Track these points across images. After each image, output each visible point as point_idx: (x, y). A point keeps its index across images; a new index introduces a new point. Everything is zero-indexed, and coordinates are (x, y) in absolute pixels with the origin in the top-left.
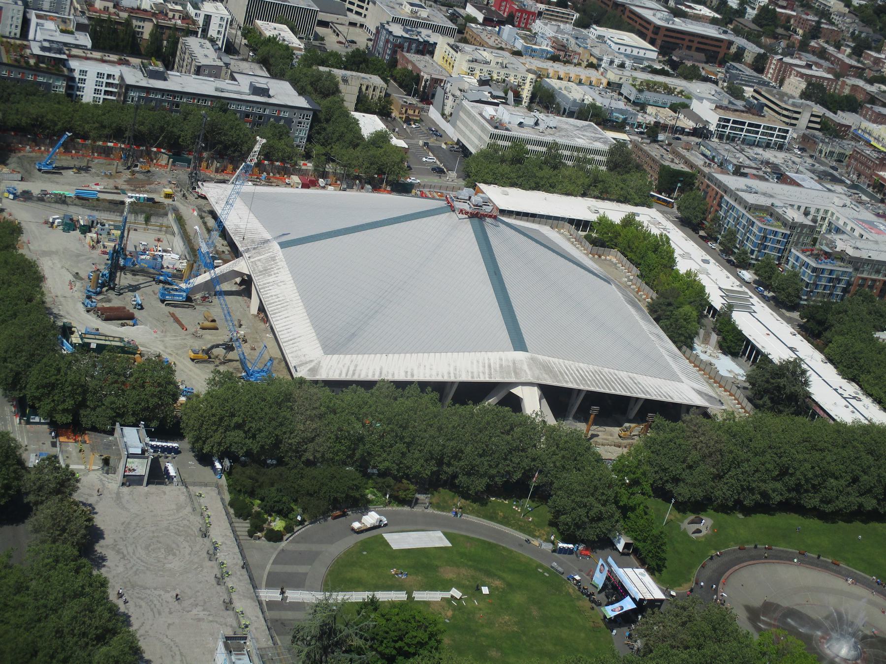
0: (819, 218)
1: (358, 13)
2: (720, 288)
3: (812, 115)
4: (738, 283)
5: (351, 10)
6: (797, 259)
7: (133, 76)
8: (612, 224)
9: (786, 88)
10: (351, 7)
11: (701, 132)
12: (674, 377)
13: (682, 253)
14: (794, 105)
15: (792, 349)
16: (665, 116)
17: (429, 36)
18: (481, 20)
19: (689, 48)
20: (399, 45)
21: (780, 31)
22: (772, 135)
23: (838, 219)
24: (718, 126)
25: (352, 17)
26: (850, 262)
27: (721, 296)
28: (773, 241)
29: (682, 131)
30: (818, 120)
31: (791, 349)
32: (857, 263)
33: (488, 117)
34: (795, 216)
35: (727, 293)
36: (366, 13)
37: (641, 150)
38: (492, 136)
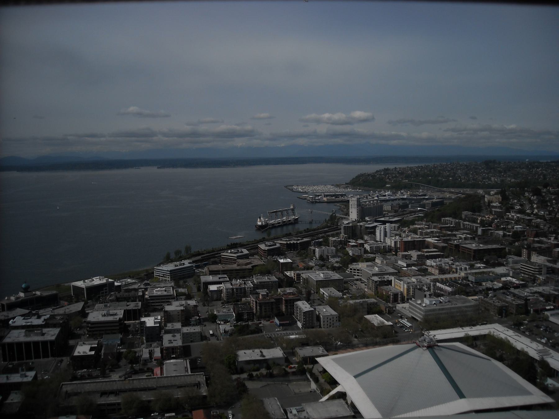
1: (358, 275)
5: (355, 275)
9: (532, 260)
10: (354, 274)
17: (388, 278)
18: (405, 266)
25: (356, 277)
27: (537, 353)
35: (539, 352)
36: (361, 274)
37: (485, 301)
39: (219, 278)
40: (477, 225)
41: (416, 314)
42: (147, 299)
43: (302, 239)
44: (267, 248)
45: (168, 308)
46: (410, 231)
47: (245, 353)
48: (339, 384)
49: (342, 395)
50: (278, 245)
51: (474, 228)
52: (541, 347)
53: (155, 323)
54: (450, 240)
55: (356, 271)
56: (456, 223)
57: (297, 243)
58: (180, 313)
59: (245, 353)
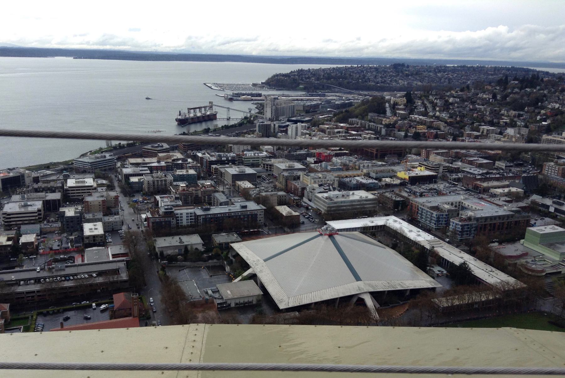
0: (457, 205)
2: (427, 240)
4: (433, 237)
6: (453, 223)
7: (199, 212)
13: (408, 230)
15: (462, 258)
16: (388, 180)
18: (313, 162)
19: (390, 154)
23: (465, 204)
28: (442, 218)
29: (396, 185)
30: (446, 168)
32: (477, 219)
34: (447, 207)
40: (381, 126)
41: (321, 206)
42: (67, 190)
47: (165, 240)
48: (251, 267)
49: (253, 277)
51: (379, 129)
53: (76, 212)
56: (361, 124)
58: (101, 203)
59: (165, 240)
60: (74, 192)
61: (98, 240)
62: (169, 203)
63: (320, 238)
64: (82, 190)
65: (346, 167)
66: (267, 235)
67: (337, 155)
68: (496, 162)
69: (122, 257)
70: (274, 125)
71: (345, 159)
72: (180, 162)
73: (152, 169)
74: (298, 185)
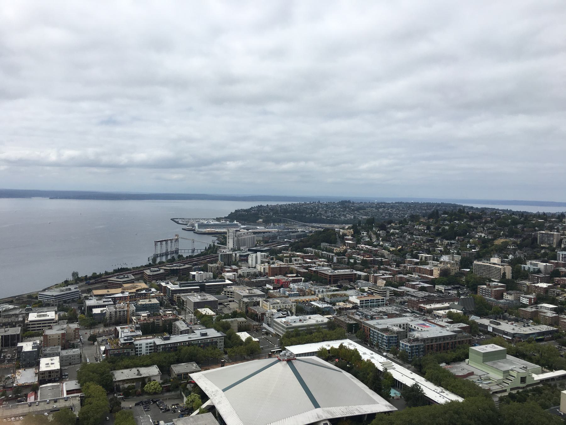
0: (405, 327)
1: (231, 297)
2: (380, 363)
3: (390, 291)
4: (386, 359)
5: (229, 297)
6: (403, 344)
7: (159, 341)
8: (336, 349)
9: (378, 285)
10: (228, 296)
11: (355, 307)
12: (374, 402)
13: (363, 353)
14: (383, 289)
15: (413, 379)
16: (341, 304)
18: (272, 289)
19: (342, 279)
20: (247, 305)
21: (370, 265)
22: (379, 302)
24: (360, 303)
25: (230, 299)
26: (422, 341)
29: (349, 309)
30: (393, 292)
31: (412, 379)
32: (424, 340)
33: (283, 322)
34: (396, 329)
38: (287, 328)
39: (104, 302)
41: (280, 331)
42: (28, 325)
43: (184, 266)
44: (151, 274)
45: (48, 332)
46: (277, 259)
47: (122, 373)
48: (210, 399)
49: (212, 409)
50: (162, 271)
51: (331, 257)
52: (383, 360)
53: (33, 348)
54: (311, 267)
55: (230, 294)
56: (315, 253)
57: (180, 269)
58: (61, 337)
60: (32, 326)
61: (54, 375)
62: (129, 334)
63: (279, 364)
64: (43, 324)
65: (302, 292)
66: (227, 362)
67: (294, 281)
68: (436, 286)
69: (77, 393)
70: (236, 254)
71: (301, 285)
72: (144, 292)
73: (115, 300)
74: (258, 310)
